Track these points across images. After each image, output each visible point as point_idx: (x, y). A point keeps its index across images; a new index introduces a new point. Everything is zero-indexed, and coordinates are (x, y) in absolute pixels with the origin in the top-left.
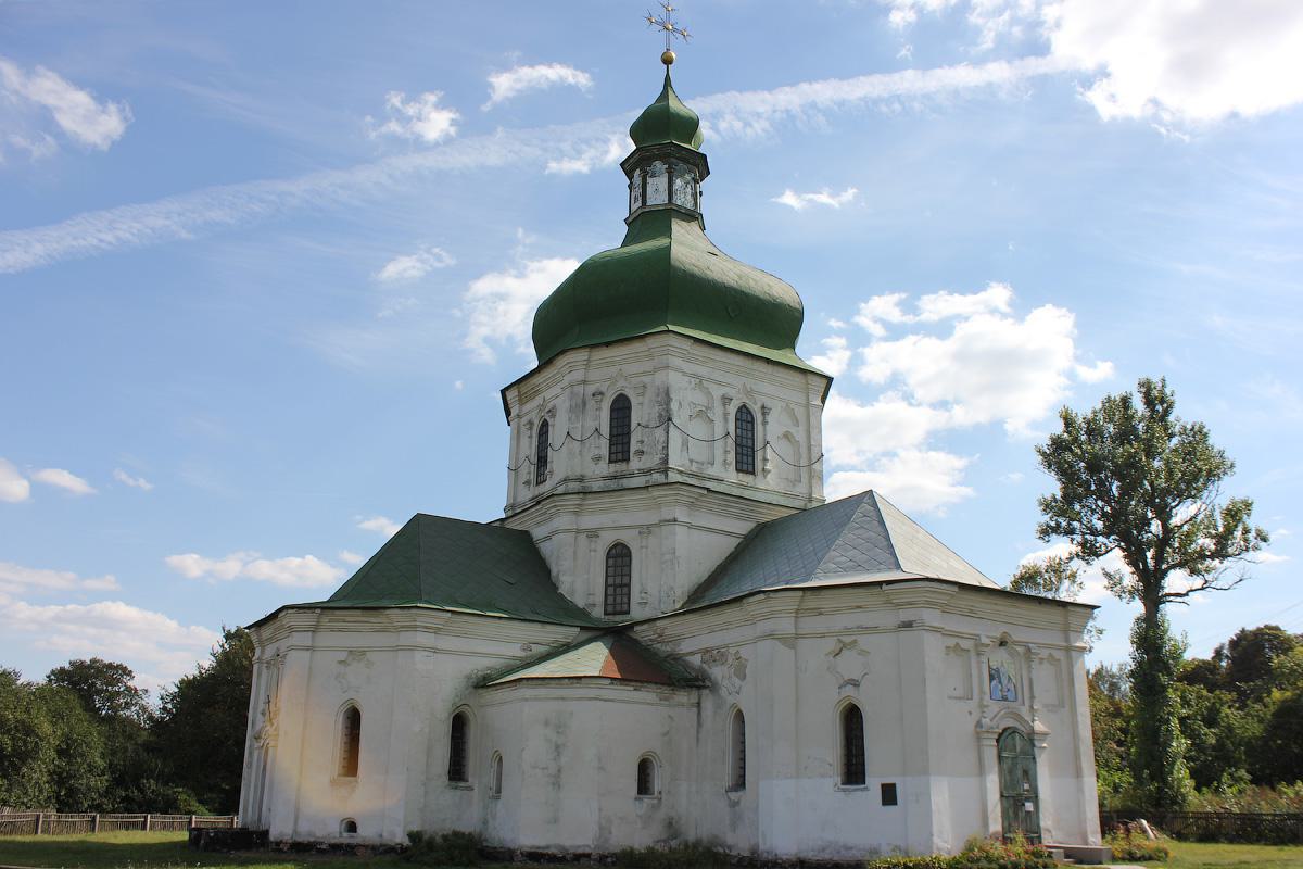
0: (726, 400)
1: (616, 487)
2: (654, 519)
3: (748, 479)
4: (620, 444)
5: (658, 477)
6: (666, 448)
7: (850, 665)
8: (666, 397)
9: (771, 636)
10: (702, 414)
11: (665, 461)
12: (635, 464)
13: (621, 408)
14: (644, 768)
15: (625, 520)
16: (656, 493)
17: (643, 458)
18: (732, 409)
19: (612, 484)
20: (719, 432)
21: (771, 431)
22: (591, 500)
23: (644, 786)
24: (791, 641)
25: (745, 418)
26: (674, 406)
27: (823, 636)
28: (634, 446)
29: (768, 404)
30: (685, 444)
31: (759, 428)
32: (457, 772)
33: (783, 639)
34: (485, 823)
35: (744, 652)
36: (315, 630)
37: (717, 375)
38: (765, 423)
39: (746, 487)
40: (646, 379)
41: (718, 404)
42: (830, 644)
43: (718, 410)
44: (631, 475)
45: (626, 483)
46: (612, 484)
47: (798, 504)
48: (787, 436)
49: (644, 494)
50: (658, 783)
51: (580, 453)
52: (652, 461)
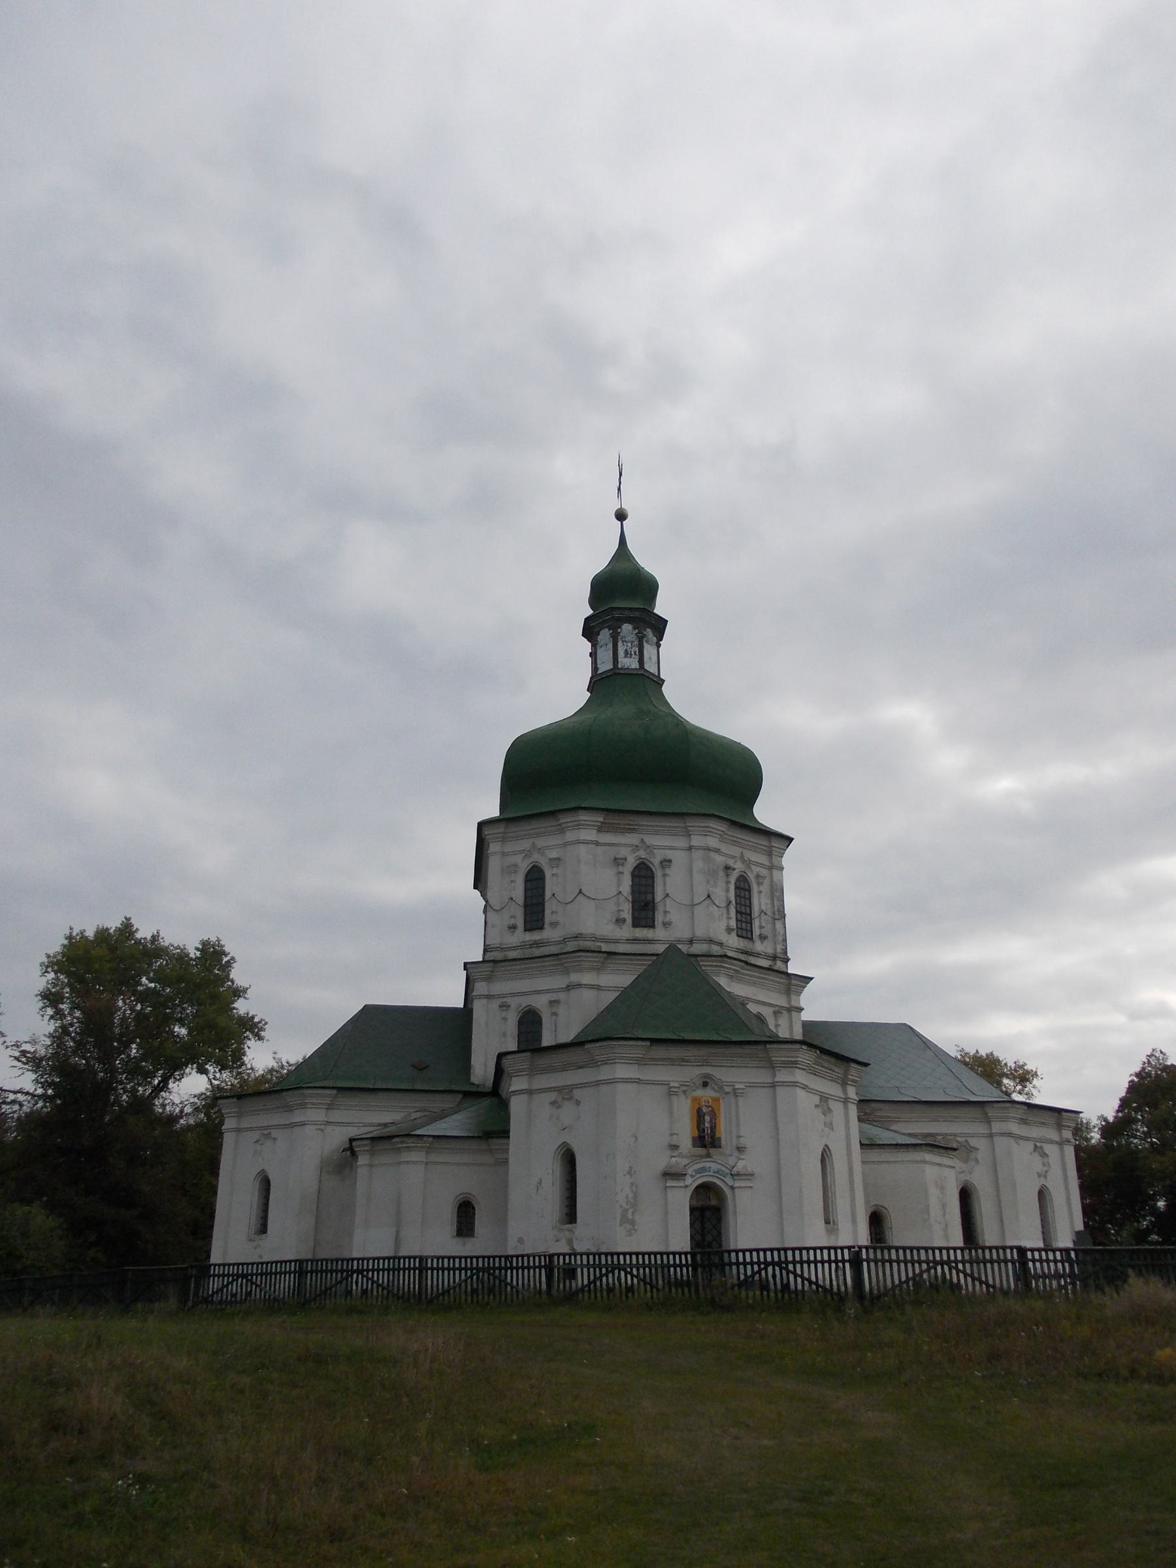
2: (781, 1001)
5: (779, 965)
6: (785, 940)
9: (1009, 1135)
13: (743, 889)
15: (763, 996)
17: (766, 942)
19: (743, 957)
27: (1027, 1139)
35: (973, 1142)
40: (764, 872)
45: (752, 960)
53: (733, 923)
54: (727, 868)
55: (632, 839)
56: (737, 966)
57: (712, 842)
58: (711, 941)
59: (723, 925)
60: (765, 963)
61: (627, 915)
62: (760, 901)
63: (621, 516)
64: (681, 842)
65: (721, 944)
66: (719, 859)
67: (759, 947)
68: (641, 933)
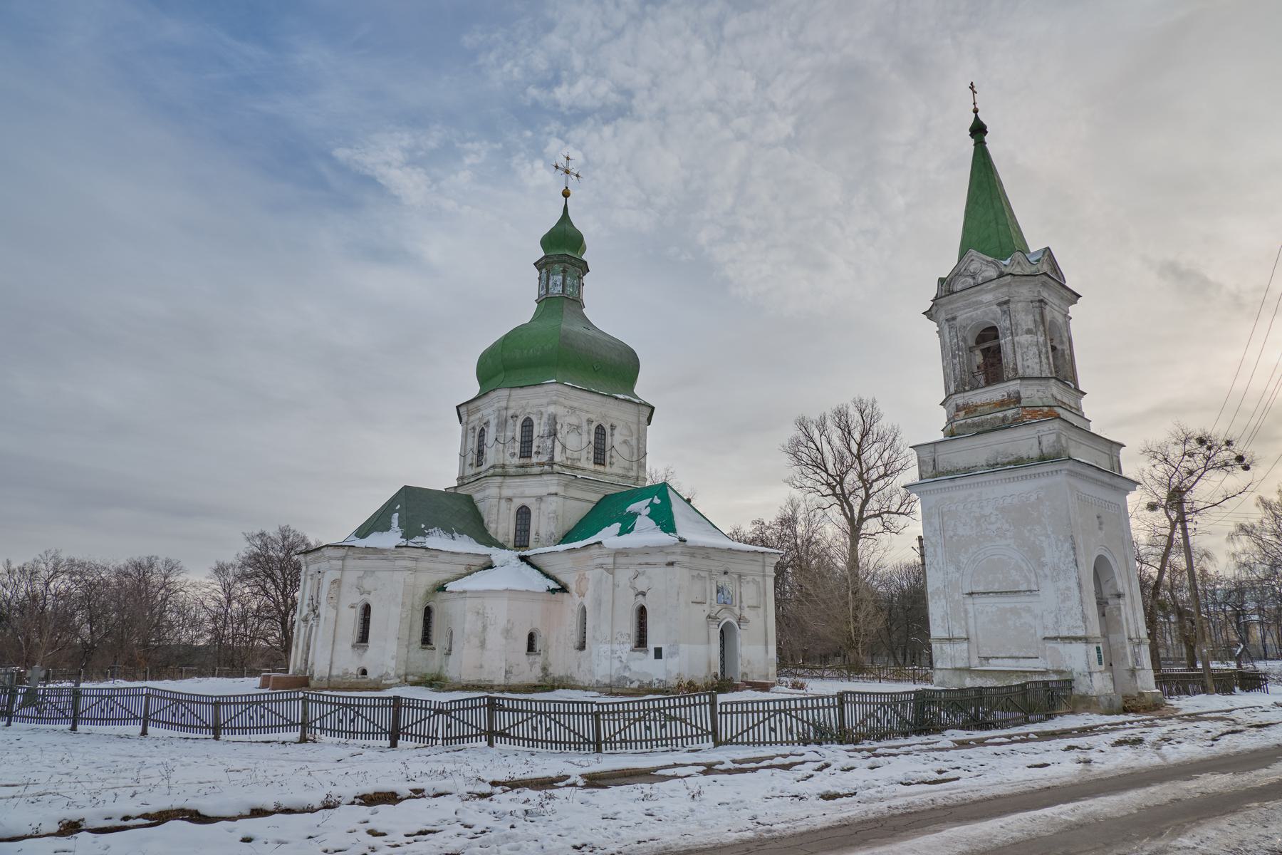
0: (590, 421)
1: (523, 472)
2: (543, 491)
3: (600, 468)
4: (526, 451)
7: (641, 584)
8: (553, 420)
9: (601, 566)
10: (577, 428)
11: (552, 458)
12: (535, 460)
14: (531, 637)
15: (528, 492)
16: (545, 477)
18: (593, 427)
20: (584, 445)
21: (616, 440)
22: (508, 481)
23: (531, 648)
24: (611, 572)
25: (600, 431)
26: (558, 427)
28: (534, 449)
29: (615, 423)
30: (564, 447)
31: (608, 439)
32: (426, 640)
33: (607, 570)
34: (441, 667)
36: (343, 558)
37: (585, 407)
38: (612, 435)
39: (600, 473)
40: (543, 409)
41: (585, 425)
42: (631, 573)
43: (585, 427)
44: (532, 466)
46: (521, 471)
47: (629, 483)
48: (625, 442)
49: (538, 479)
50: (538, 646)
51: (500, 453)
52: (545, 458)
53: (517, 451)
54: (514, 417)
55: (479, 415)
56: (499, 479)
57: (504, 404)
58: (494, 467)
59: (507, 454)
60: (536, 470)
61: (475, 462)
62: (539, 429)
63: (566, 194)
64: (490, 411)
65: (503, 466)
66: (511, 412)
67: (535, 460)
68: (480, 469)
